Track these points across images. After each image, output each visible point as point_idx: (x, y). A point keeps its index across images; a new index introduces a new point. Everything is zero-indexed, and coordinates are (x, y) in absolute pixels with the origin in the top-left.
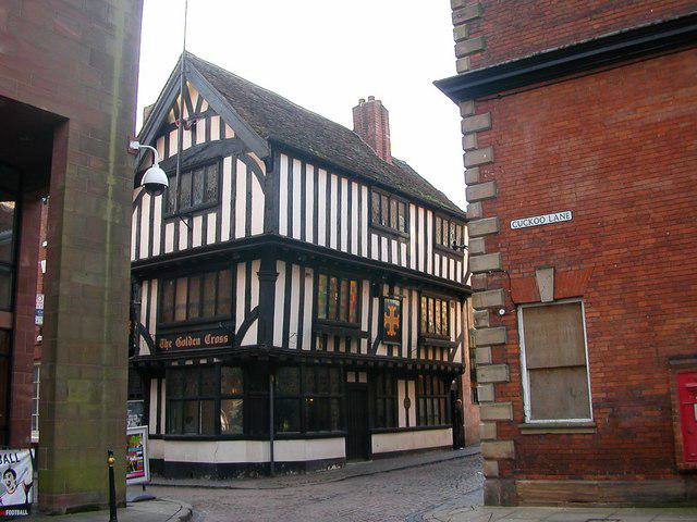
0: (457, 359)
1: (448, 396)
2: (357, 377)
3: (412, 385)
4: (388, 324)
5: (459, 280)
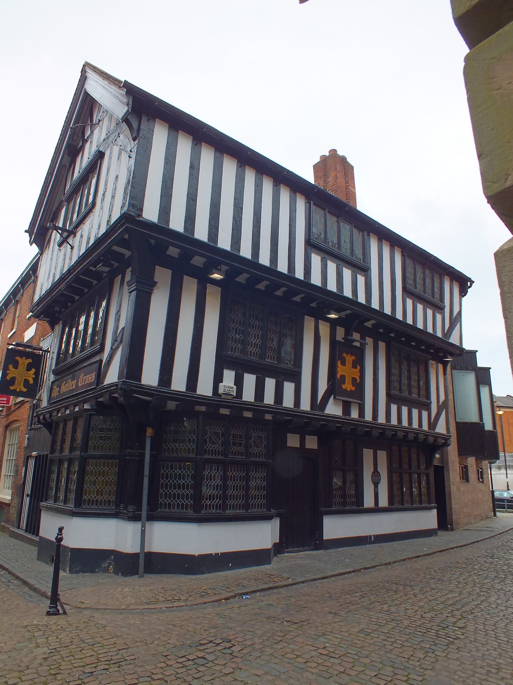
0: (441, 428)
1: (431, 472)
2: (302, 442)
3: (382, 455)
4: (343, 377)
5: (439, 334)
